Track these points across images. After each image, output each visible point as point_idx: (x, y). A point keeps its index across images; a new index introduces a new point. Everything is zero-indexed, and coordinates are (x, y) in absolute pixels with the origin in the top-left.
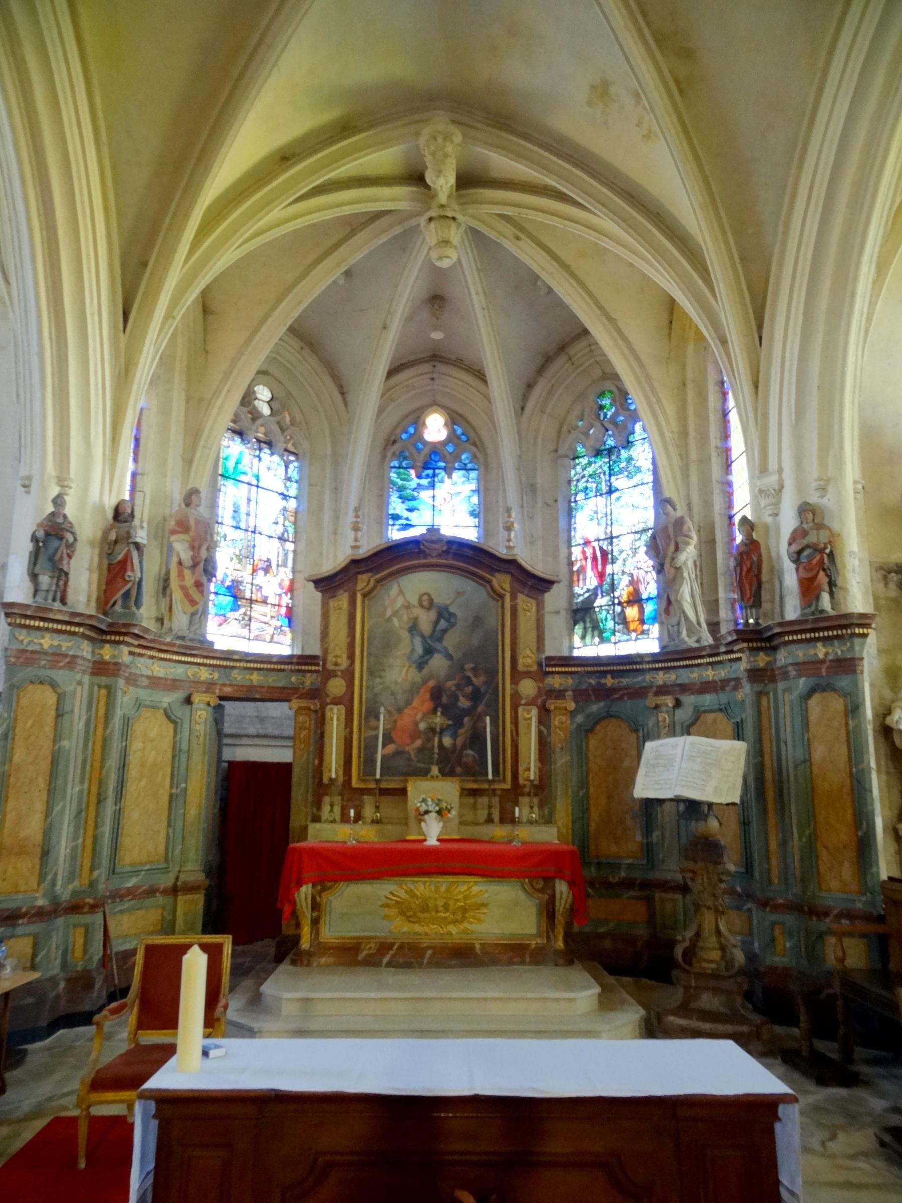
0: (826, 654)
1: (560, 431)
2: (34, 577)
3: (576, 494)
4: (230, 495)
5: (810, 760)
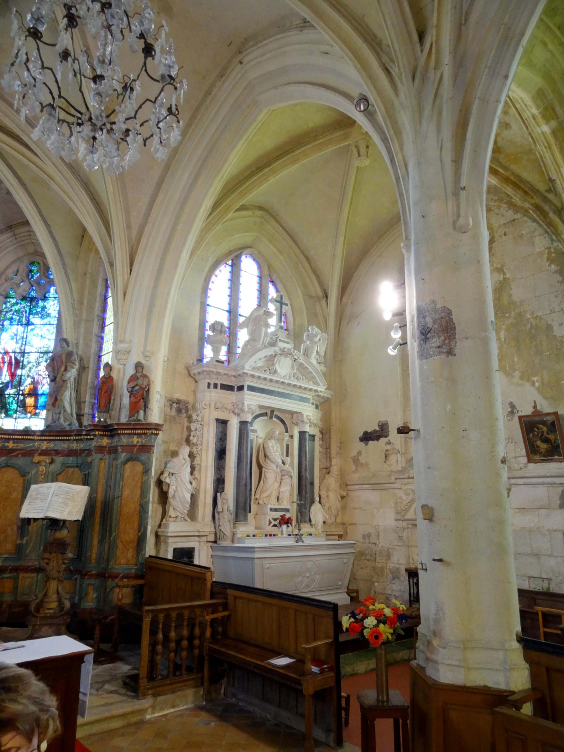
0: (138, 442)
3: (4, 320)
5: (121, 496)
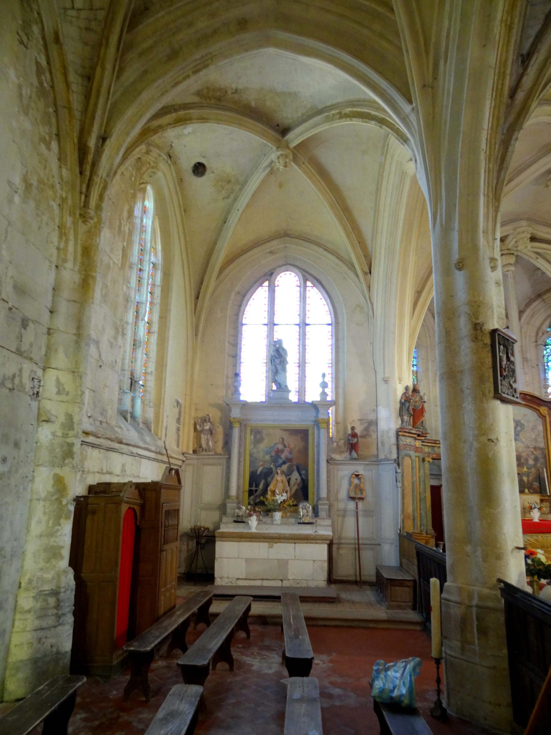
1: (537, 334)
3: (548, 362)
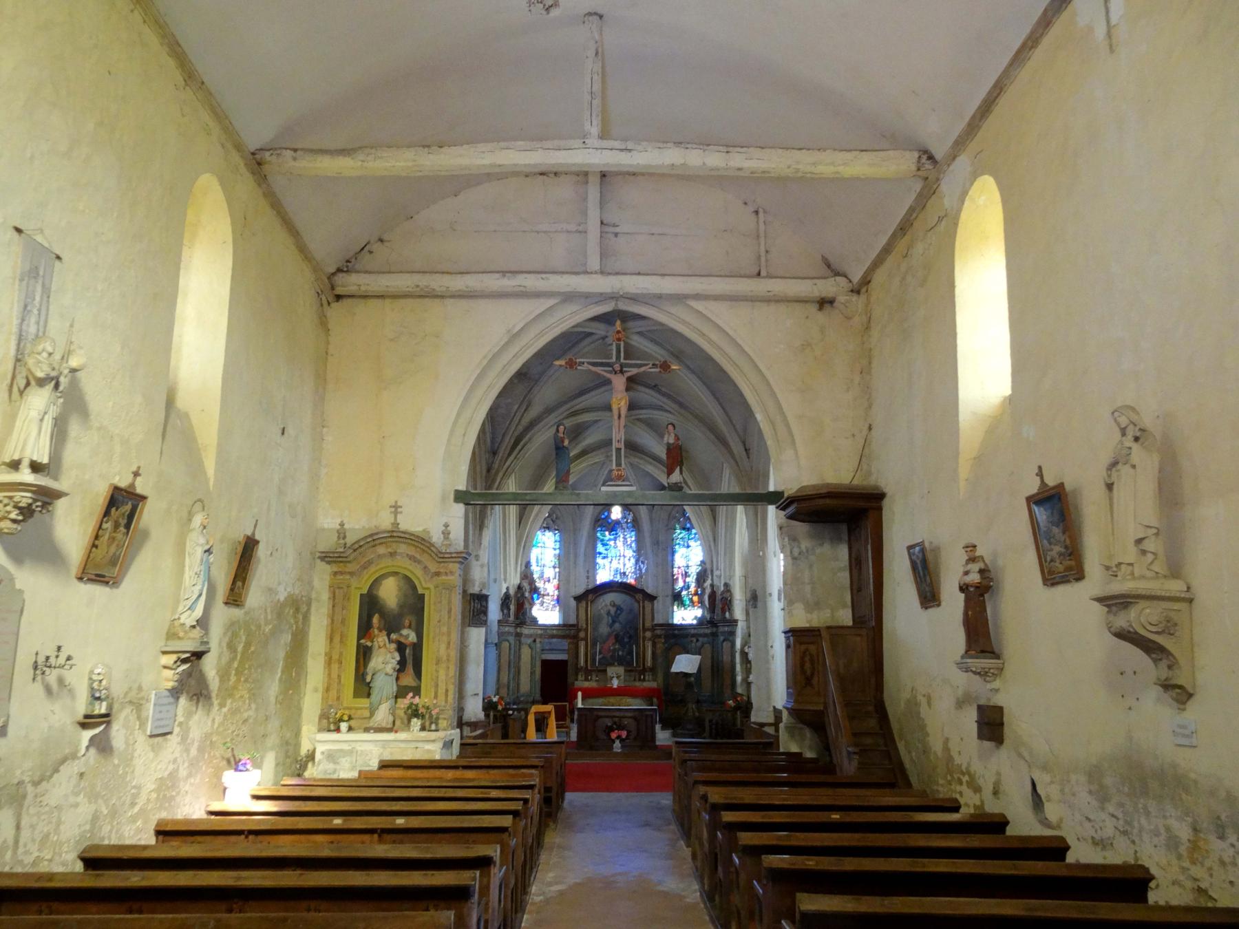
2: (502, 610)
4: (534, 554)
